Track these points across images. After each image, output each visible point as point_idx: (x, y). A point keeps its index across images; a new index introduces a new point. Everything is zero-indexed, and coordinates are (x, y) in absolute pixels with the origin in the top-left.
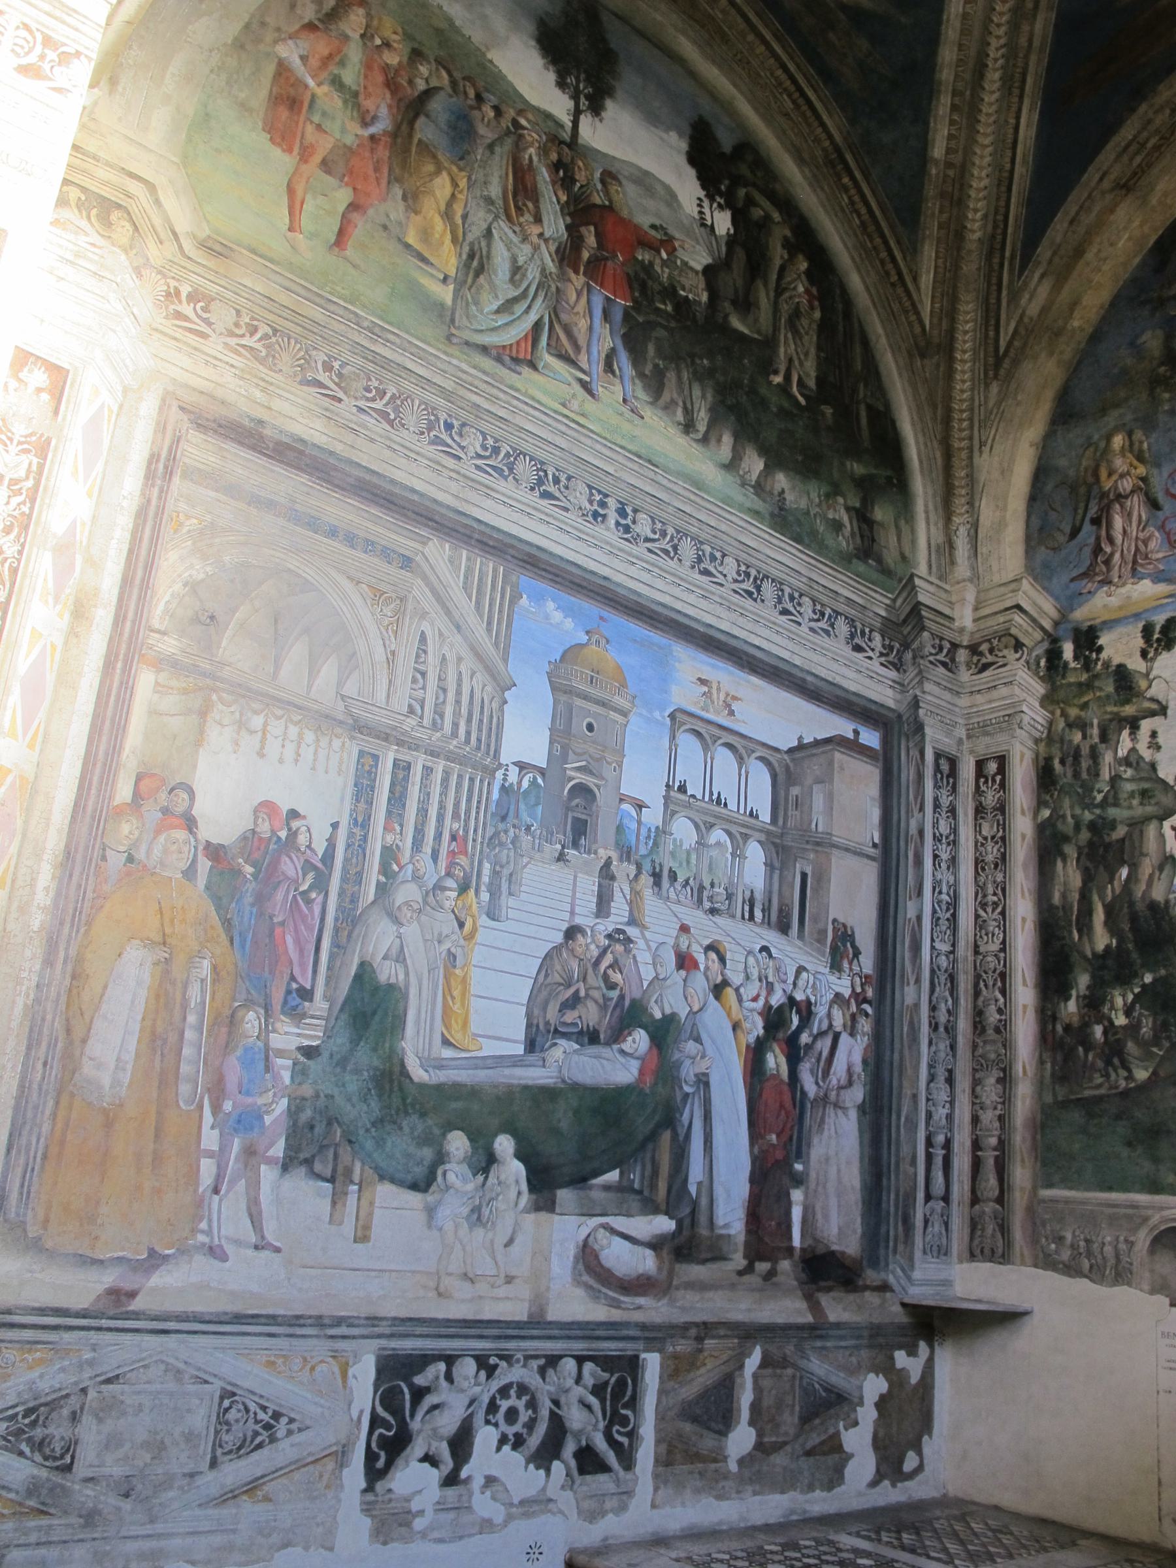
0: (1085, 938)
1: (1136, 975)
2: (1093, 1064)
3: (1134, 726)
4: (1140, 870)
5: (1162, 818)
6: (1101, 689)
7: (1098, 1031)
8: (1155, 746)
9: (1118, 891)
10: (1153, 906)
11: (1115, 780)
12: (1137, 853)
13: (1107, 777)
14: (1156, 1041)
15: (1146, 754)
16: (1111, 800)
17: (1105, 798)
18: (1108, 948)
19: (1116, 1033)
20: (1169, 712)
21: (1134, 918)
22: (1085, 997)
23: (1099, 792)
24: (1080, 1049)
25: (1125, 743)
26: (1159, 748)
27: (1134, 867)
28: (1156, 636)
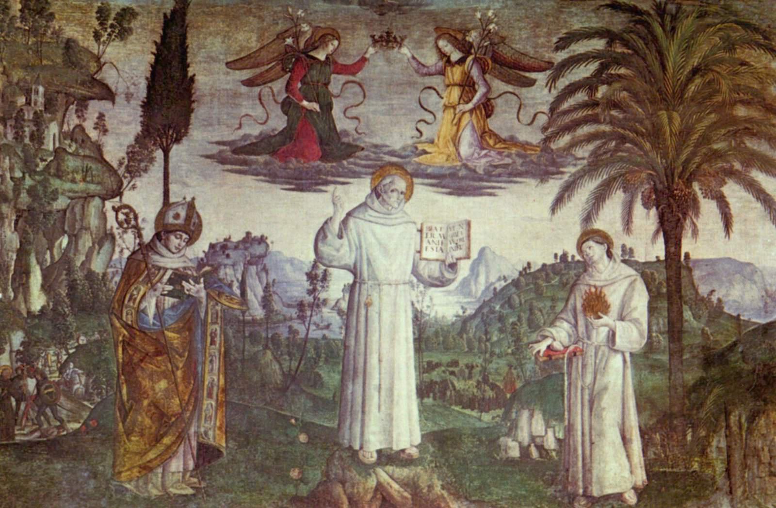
0: (21, 297)
1: (71, 337)
2: (26, 413)
3: (82, 104)
4: (81, 242)
5: (104, 199)
6: (48, 58)
7: (31, 384)
8: (101, 126)
9: (57, 258)
10: (90, 275)
11: (59, 152)
12: (77, 226)
13: (51, 148)
14: (88, 396)
15: (93, 134)
16: (52, 171)
17: (48, 167)
18: (43, 310)
19: (46, 388)
20: (117, 99)
21: (72, 287)
22: (18, 352)
23: (42, 160)
24: (13, 399)
25: (73, 120)
26: (105, 131)
27: (74, 238)
28: (110, 22)
